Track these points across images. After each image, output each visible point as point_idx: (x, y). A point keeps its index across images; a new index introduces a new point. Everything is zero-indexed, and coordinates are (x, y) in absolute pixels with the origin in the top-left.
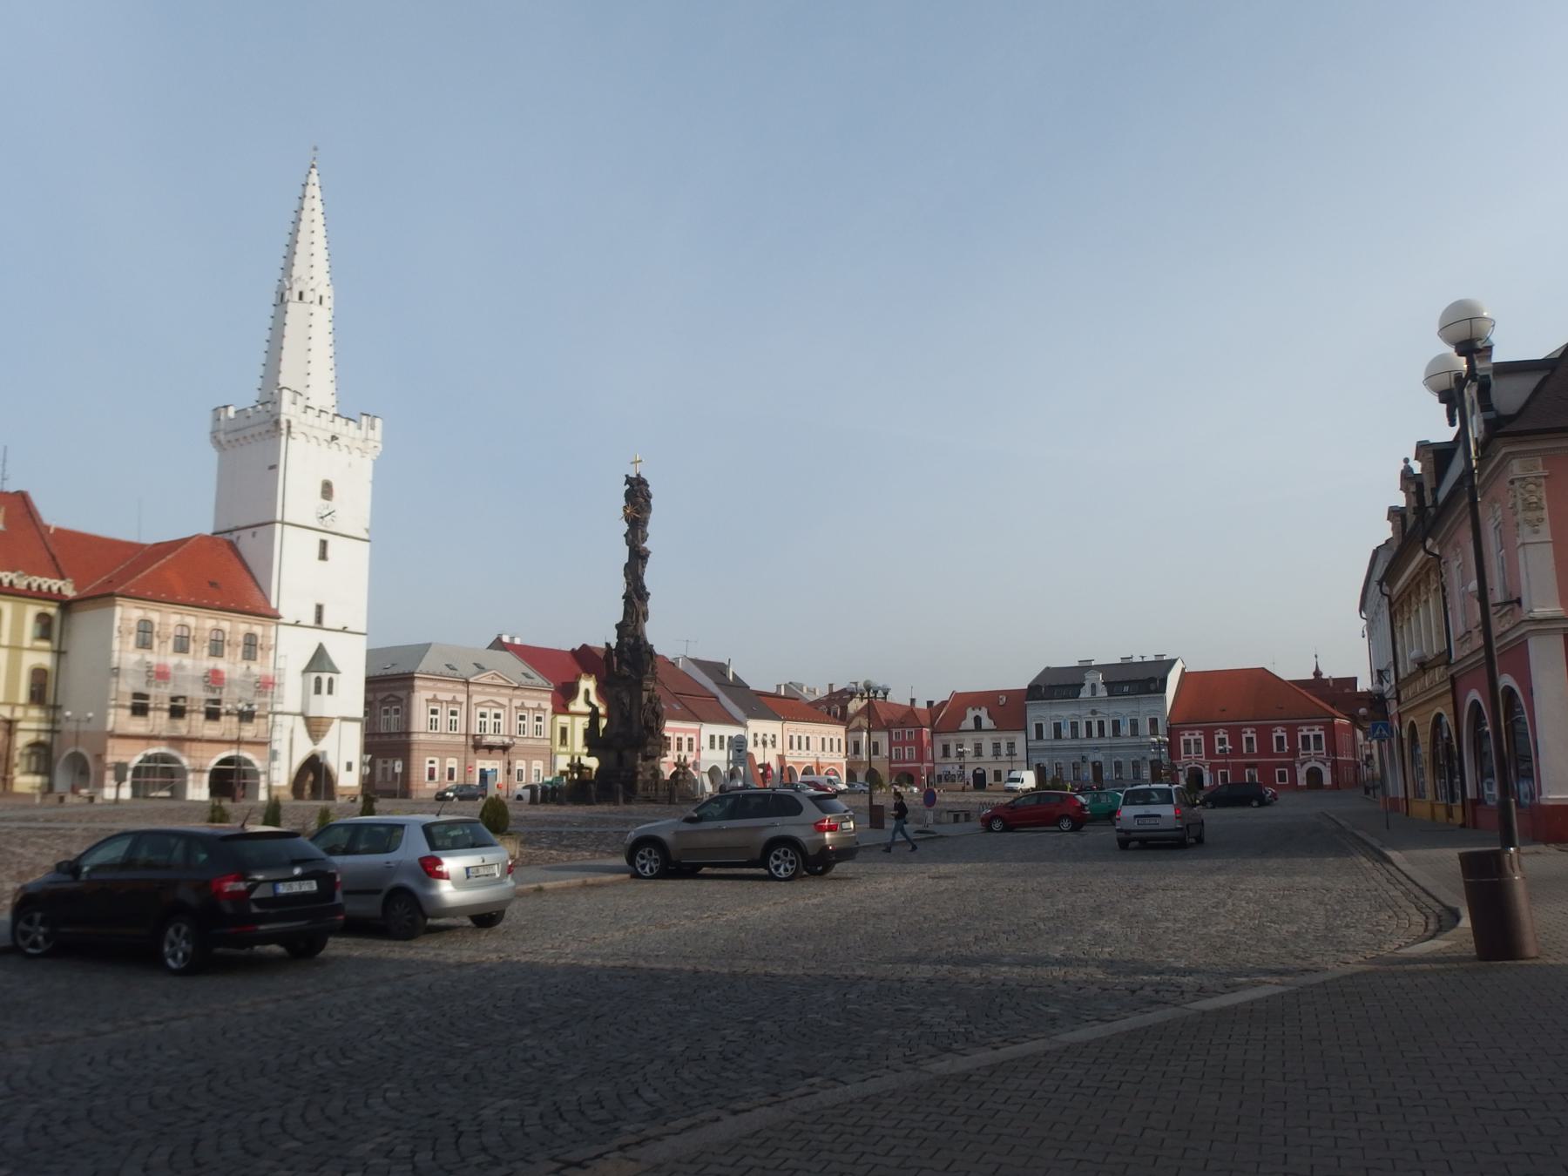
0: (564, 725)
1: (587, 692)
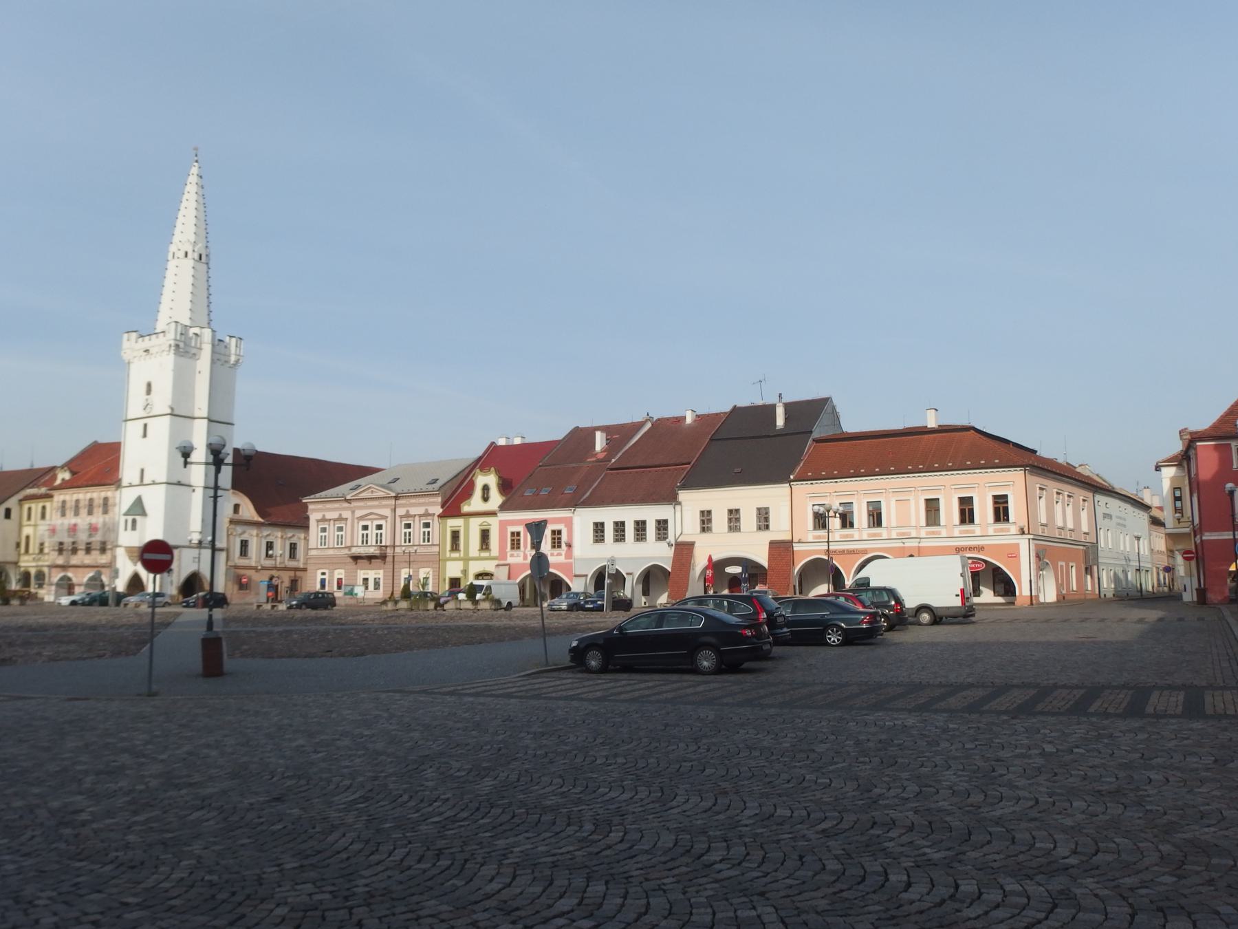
1: (486, 488)
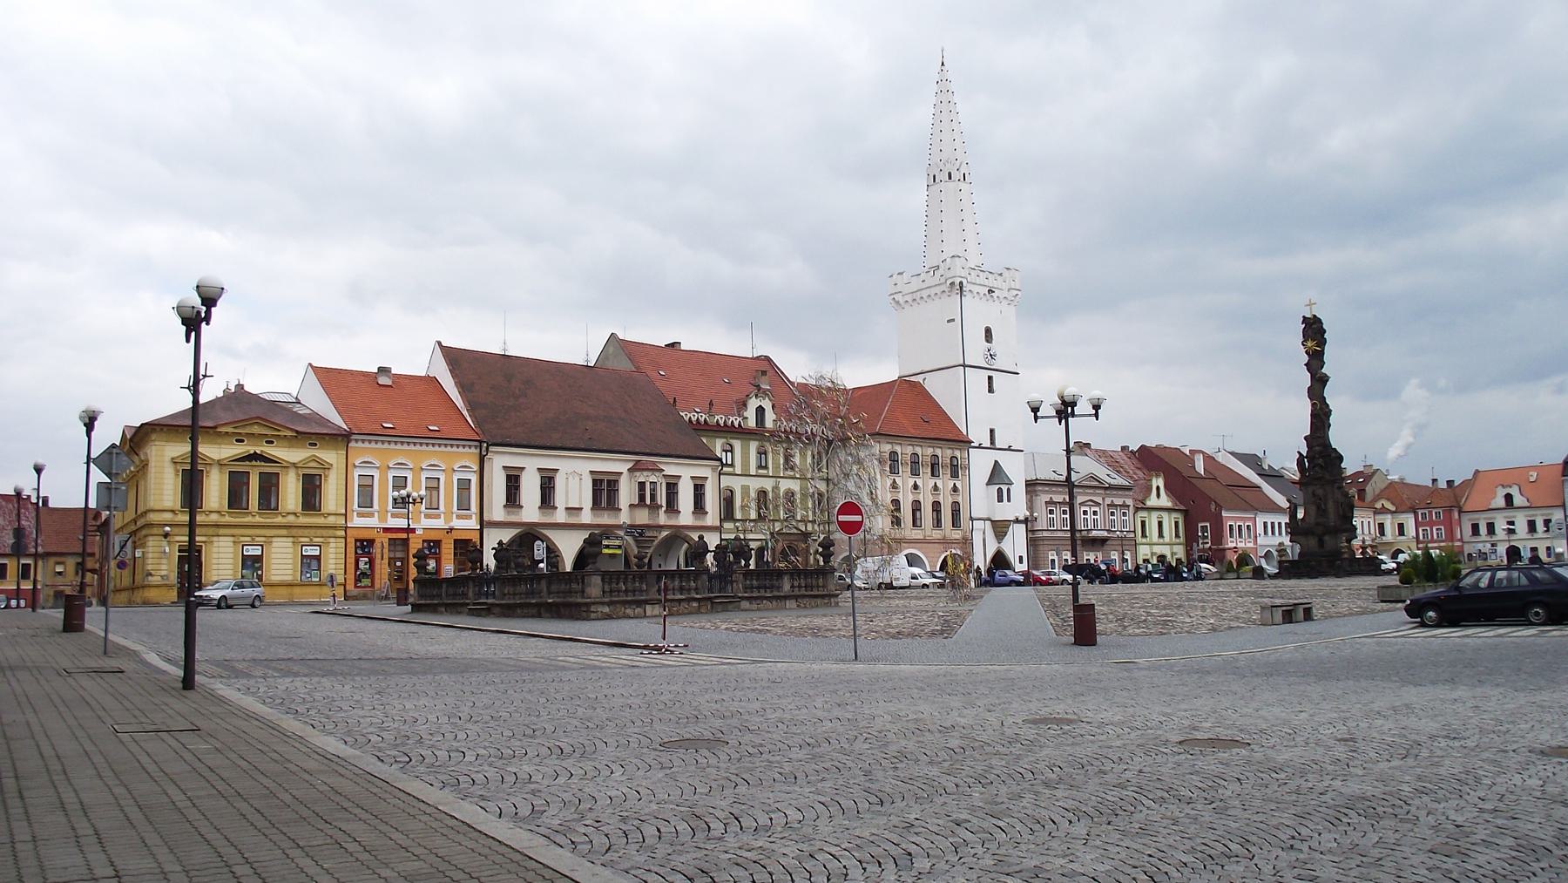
0: (1143, 519)
1: (1158, 488)
